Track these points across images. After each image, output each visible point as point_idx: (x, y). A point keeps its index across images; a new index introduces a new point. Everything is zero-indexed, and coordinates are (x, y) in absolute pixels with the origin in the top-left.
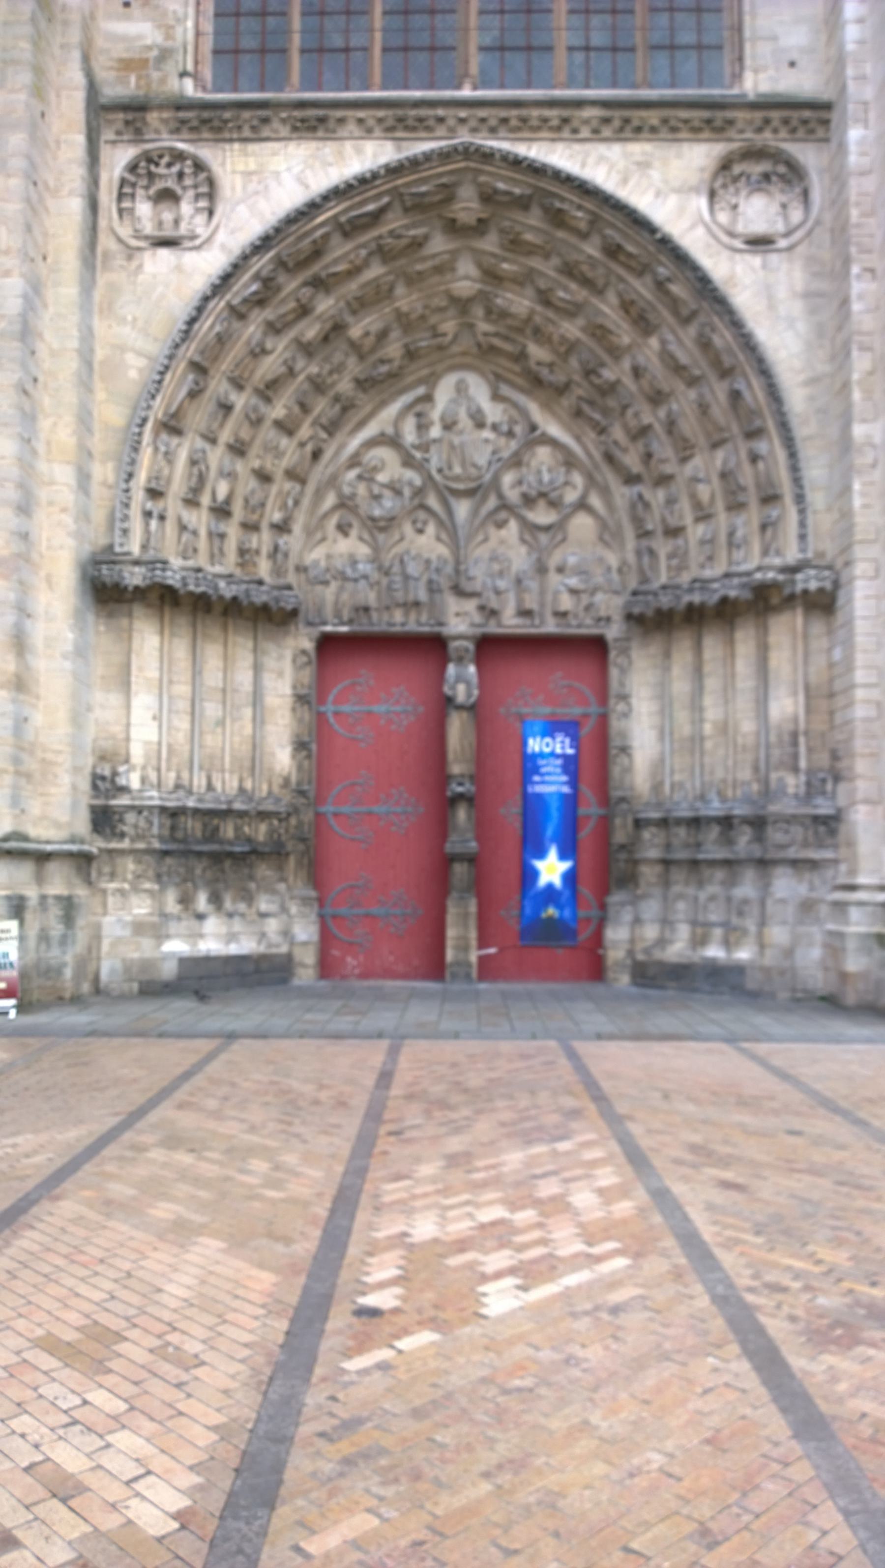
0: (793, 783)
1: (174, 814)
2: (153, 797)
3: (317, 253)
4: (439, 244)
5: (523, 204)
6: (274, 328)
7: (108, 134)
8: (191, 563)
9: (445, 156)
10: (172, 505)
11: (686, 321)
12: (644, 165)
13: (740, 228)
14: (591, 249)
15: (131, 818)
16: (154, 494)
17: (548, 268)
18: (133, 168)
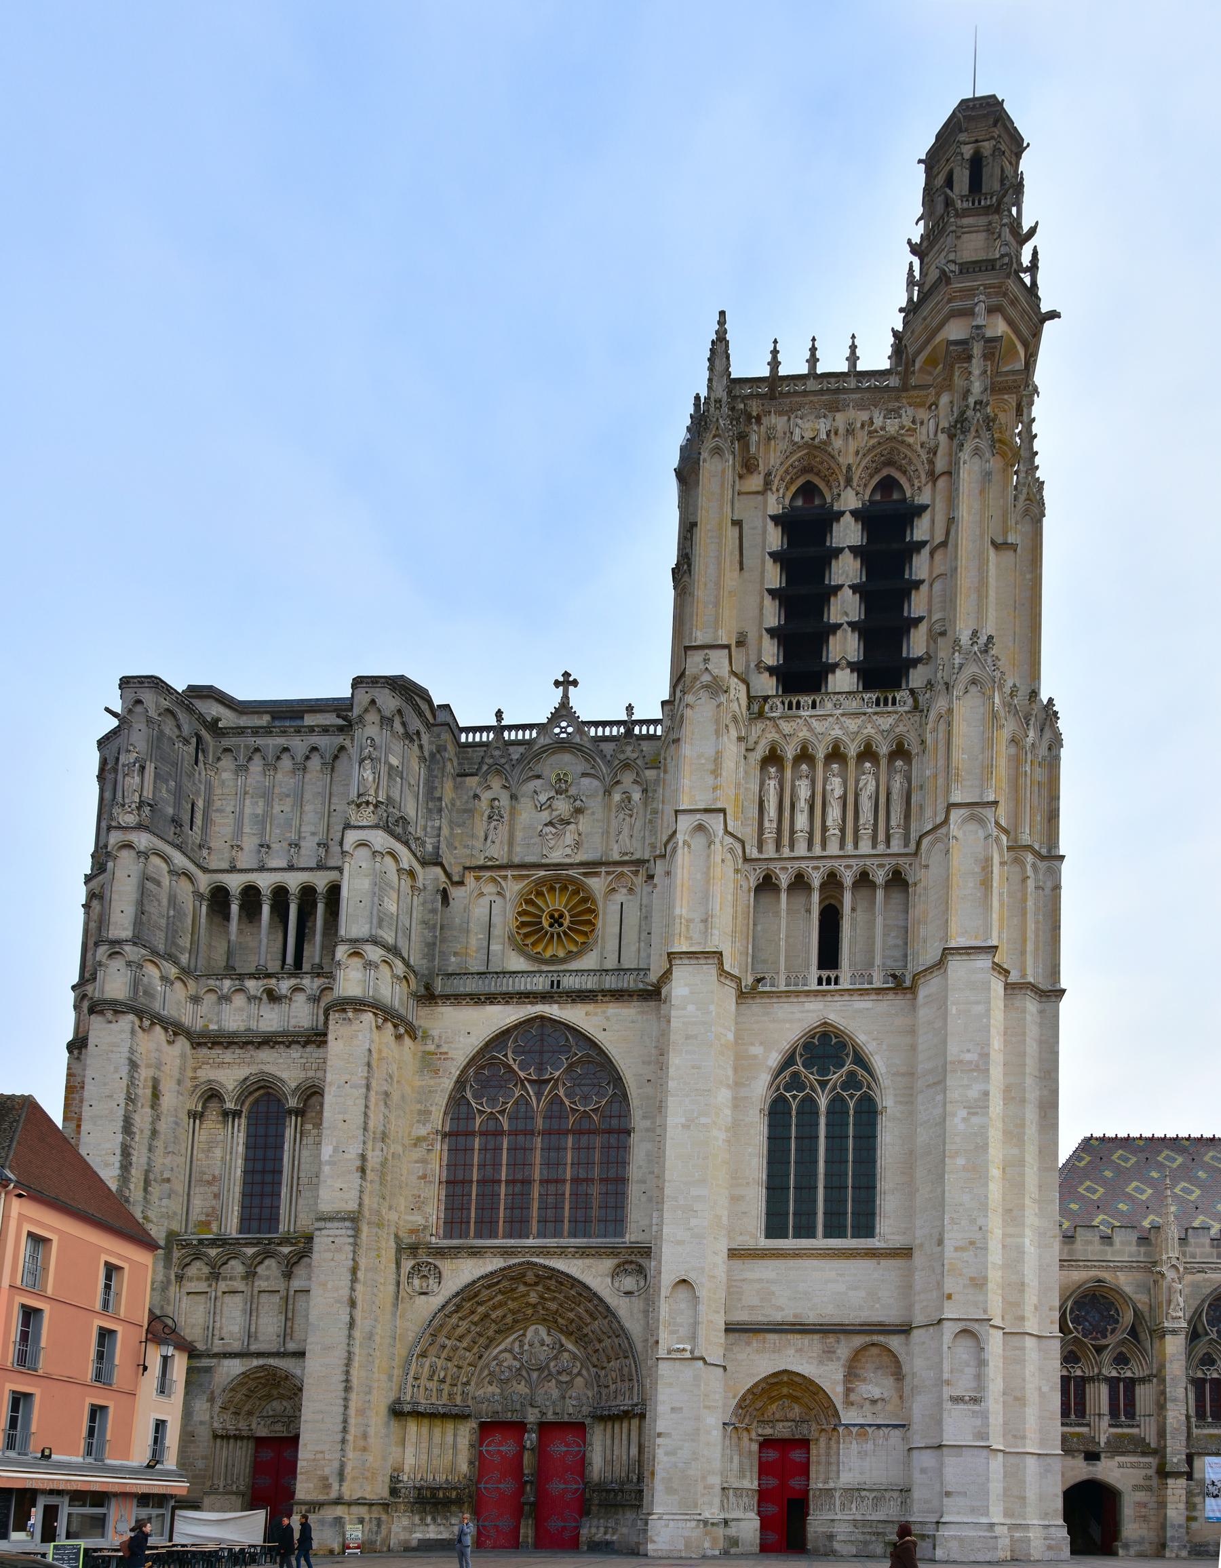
0: (635, 1478)
1: (419, 1489)
2: (411, 1484)
3: (476, 1296)
4: (522, 1288)
5: (550, 1278)
6: (461, 1319)
7: (404, 1256)
8: (429, 1402)
9: (520, 1264)
10: (423, 1381)
11: (605, 1317)
12: (591, 1267)
13: (622, 1289)
14: (573, 1292)
15: (403, 1491)
16: (416, 1379)
17: (561, 1296)
18: (413, 1268)
